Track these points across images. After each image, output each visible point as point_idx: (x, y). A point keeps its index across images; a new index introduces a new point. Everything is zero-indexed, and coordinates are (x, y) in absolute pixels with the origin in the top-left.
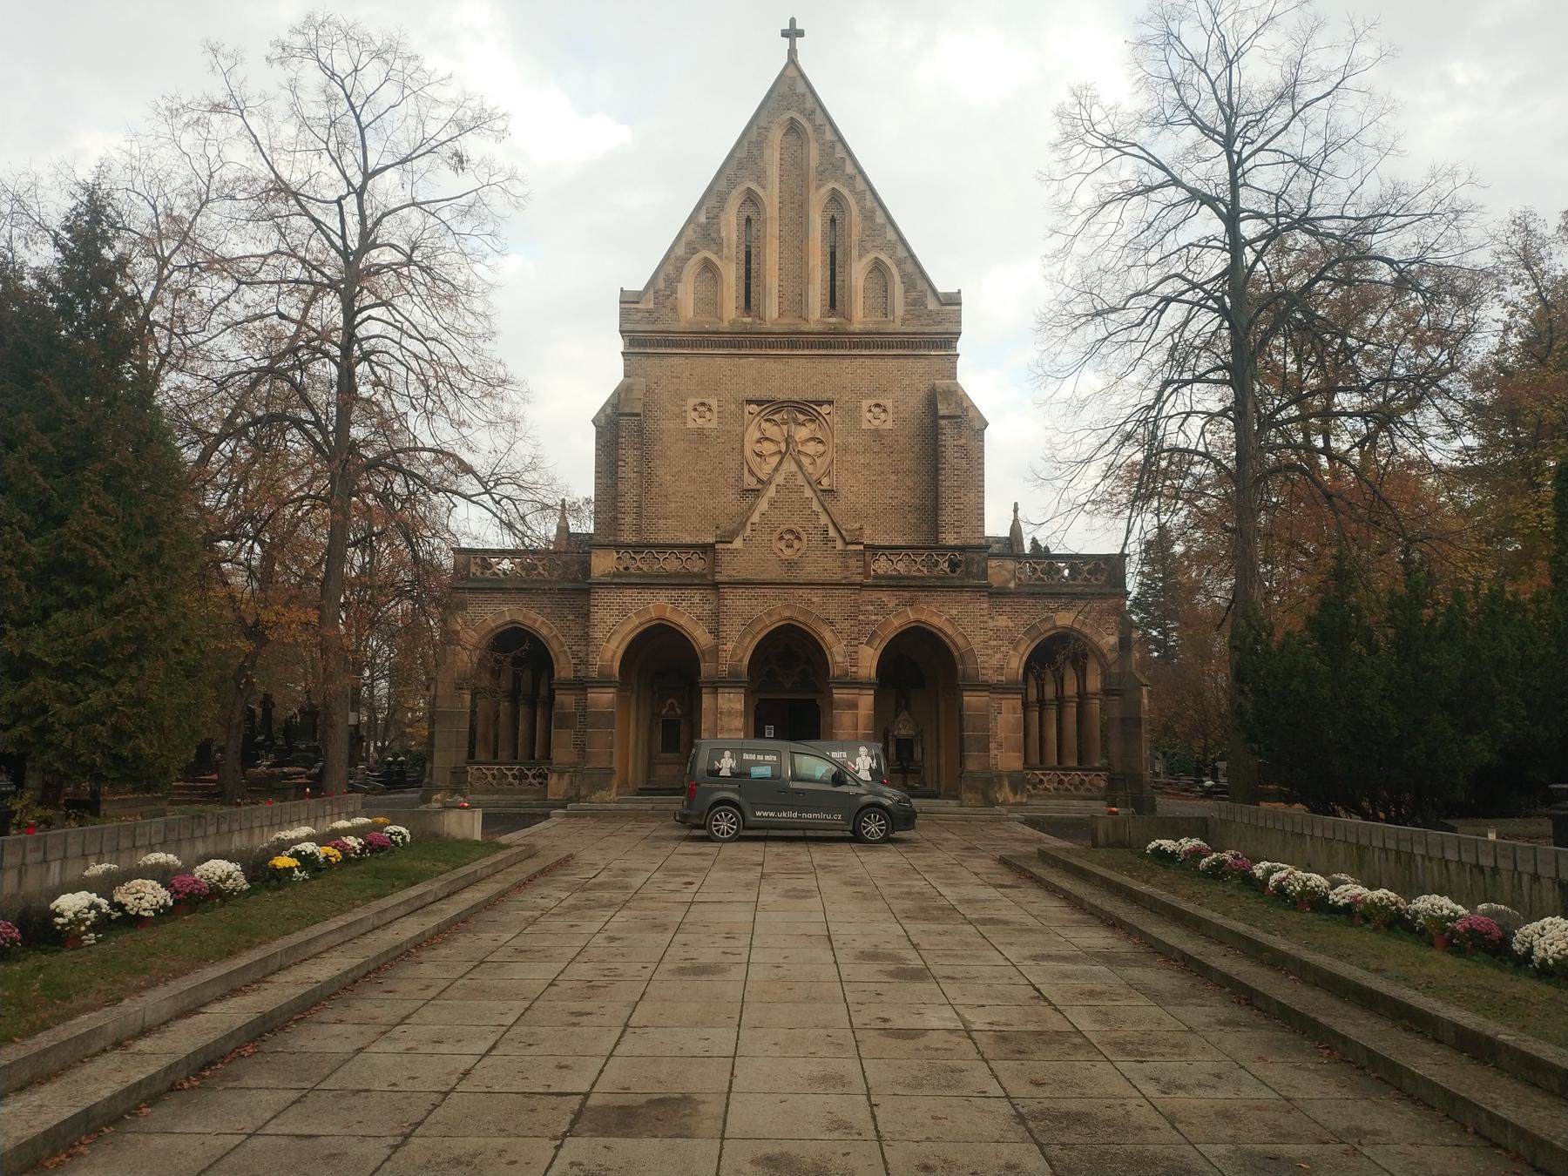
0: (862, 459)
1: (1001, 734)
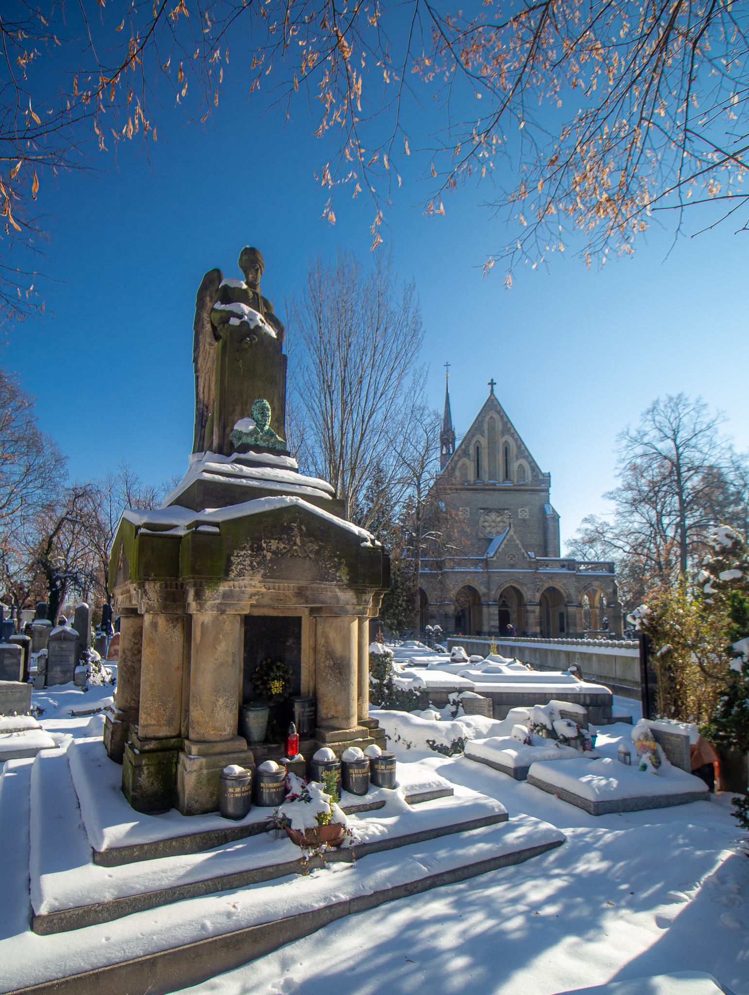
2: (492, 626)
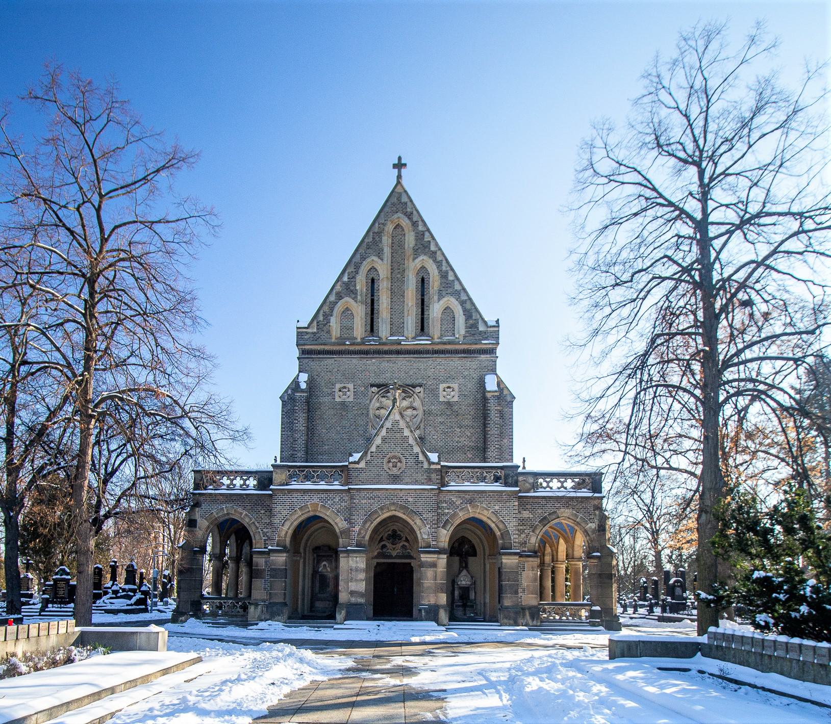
0: (440, 419)
1: (525, 583)
2: (352, 593)
